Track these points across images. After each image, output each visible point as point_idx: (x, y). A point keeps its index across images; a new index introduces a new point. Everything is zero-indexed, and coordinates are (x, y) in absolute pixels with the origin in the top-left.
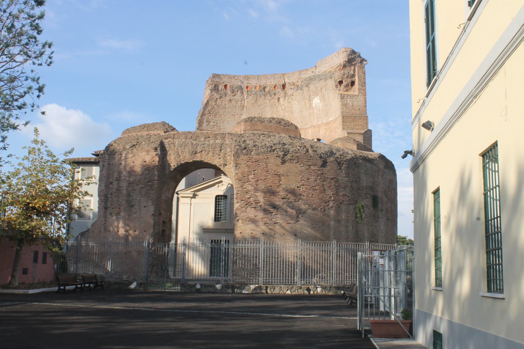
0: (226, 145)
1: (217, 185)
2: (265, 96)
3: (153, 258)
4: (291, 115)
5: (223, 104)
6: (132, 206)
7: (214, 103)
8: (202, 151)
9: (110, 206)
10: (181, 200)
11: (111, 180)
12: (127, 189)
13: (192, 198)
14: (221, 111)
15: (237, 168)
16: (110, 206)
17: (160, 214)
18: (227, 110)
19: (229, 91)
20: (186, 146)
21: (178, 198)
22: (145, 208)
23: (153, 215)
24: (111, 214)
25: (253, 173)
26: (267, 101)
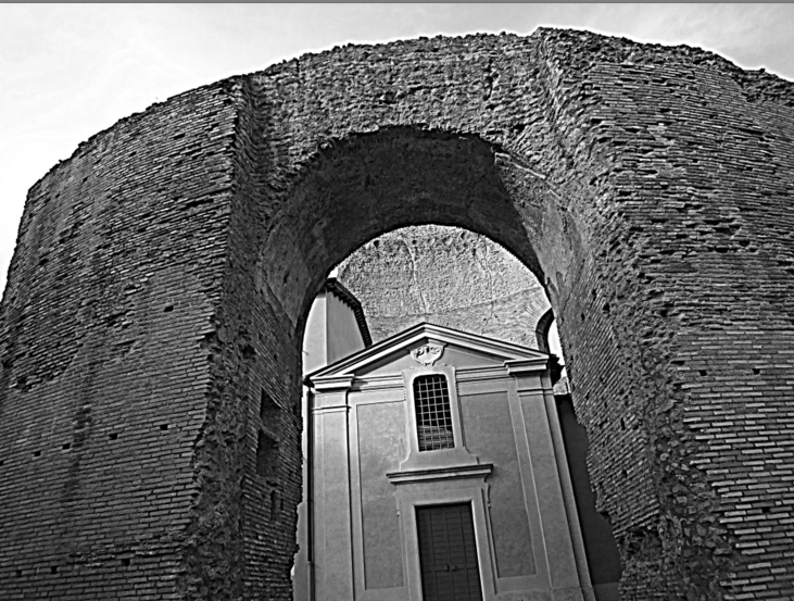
0: (509, 60)
1: (416, 351)
2: (448, 251)
3: (207, 581)
4: (501, 274)
5: (375, 270)
6: (111, 321)
7: (359, 270)
8: (413, 91)
9: (23, 349)
10: (321, 401)
11: (42, 249)
12: (97, 256)
13: (349, 390)
14: (373, 283)
15: (590, 101)
16: (23, 349)
17: (248, 351)
18: (383, 280)
19: (382, 249)
20: (344, 81)
21: (311, 395)
22: (170, 315)
23: (208, 336)
24: (22, 380)
25: (659, 117)
26: (454, 258)
